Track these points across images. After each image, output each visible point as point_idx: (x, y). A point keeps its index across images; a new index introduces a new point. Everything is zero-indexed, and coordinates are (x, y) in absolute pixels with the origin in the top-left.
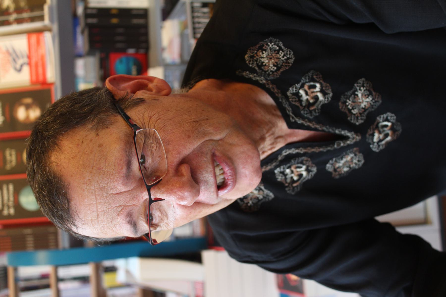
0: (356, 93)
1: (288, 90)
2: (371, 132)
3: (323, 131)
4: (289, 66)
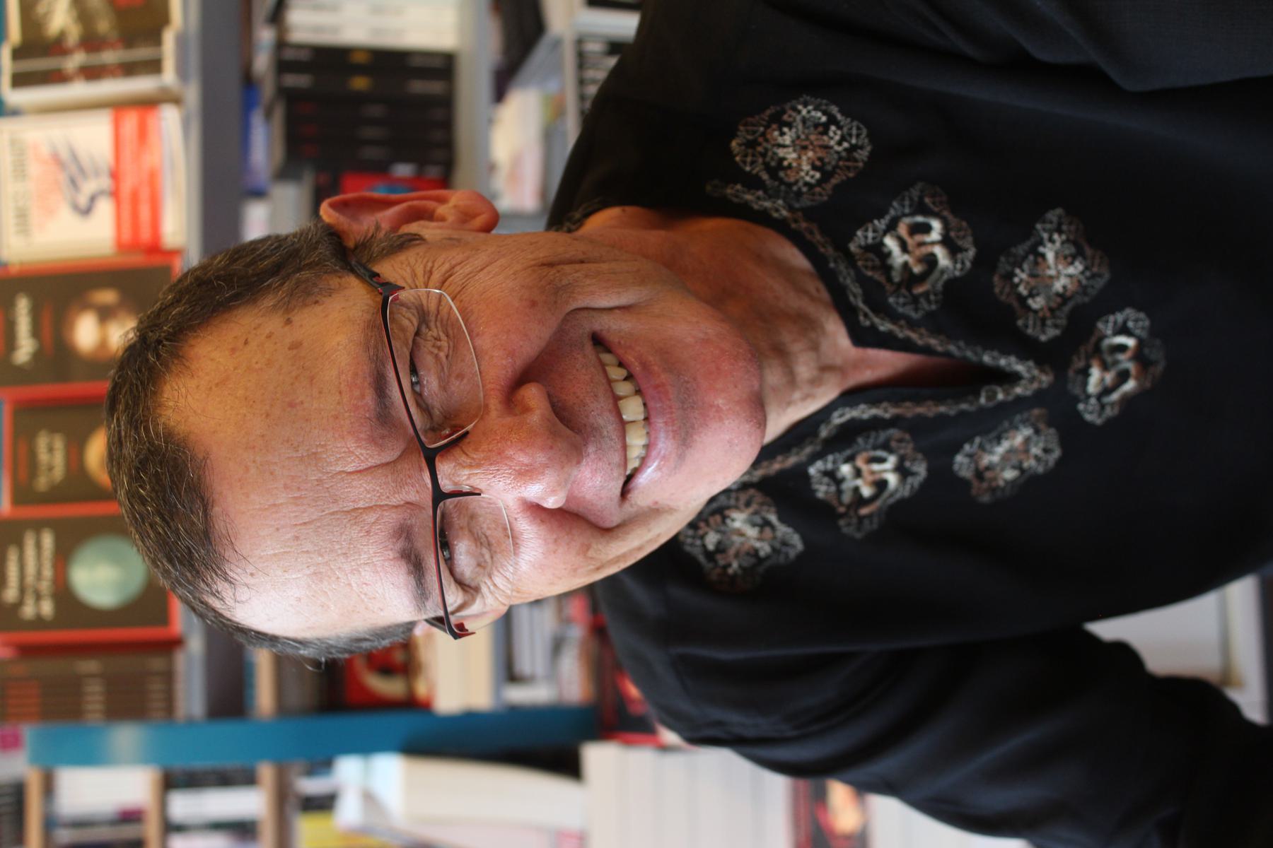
0: (1041, 249)
1: (852, 236)
2: (1081, 364)
3: (947, 354)
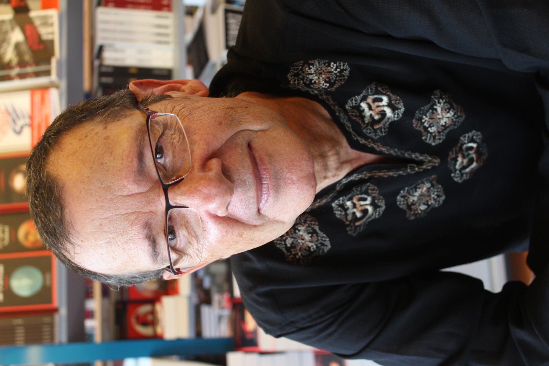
0: (435, 107)
1: (346, 103)
4: (344, 79)
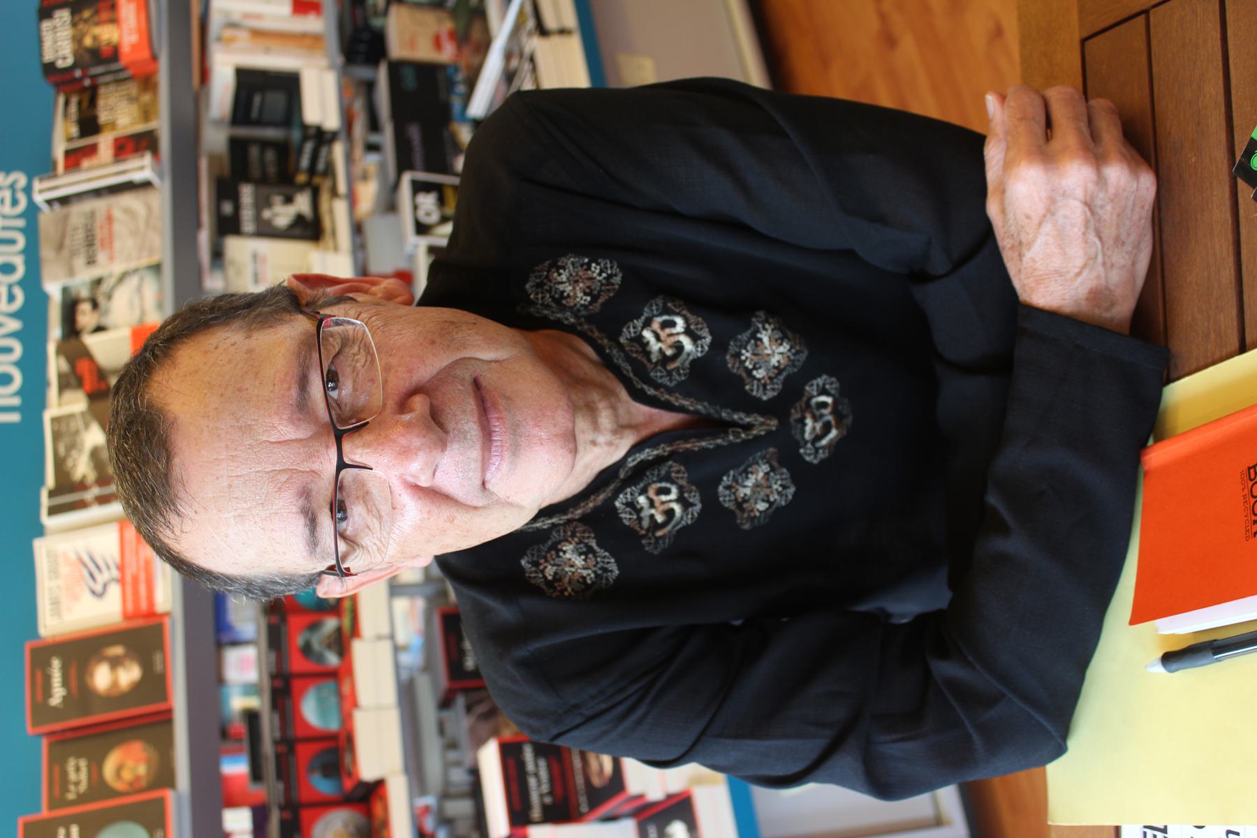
2: (798, 416)
